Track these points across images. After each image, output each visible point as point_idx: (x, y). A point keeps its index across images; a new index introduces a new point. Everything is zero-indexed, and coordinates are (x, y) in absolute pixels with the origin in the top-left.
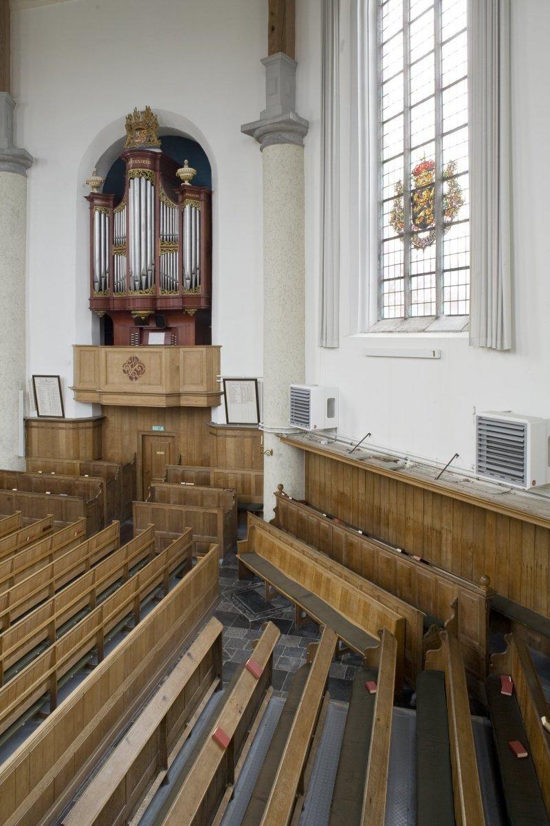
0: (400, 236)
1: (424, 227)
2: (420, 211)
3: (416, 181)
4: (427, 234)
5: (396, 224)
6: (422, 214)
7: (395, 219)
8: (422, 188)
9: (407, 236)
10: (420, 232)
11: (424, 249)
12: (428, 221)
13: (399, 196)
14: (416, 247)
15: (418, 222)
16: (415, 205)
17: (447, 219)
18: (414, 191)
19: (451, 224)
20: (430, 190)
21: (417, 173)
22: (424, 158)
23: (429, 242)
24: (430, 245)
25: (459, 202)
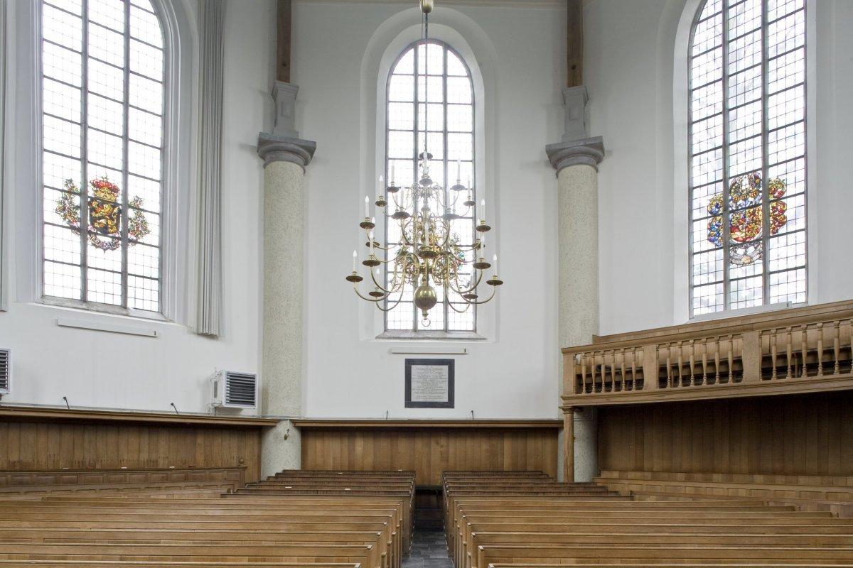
0: (72, 228)
1: (105, 230)
2: (100, 218)
3: (96, 191)
4: (108, 240)
5: (65, 215)
6: (103, 221)
7: (64, 209)
8: (104, 202)
9: (83, 232)
10: (100, 235)
11: (105, 250)
12: (110, 230)
13: (71, 192)
14: (94, 245)
15: (96, 225)
16: (93, 210)
17: (130, 236)
18: (92, 199)
19: (136, 242)
20: (114, 207)
21: (97, 185)
22: (106, 178)
23: (113, 246)
24: (113, 249)
25: (145, 230)
